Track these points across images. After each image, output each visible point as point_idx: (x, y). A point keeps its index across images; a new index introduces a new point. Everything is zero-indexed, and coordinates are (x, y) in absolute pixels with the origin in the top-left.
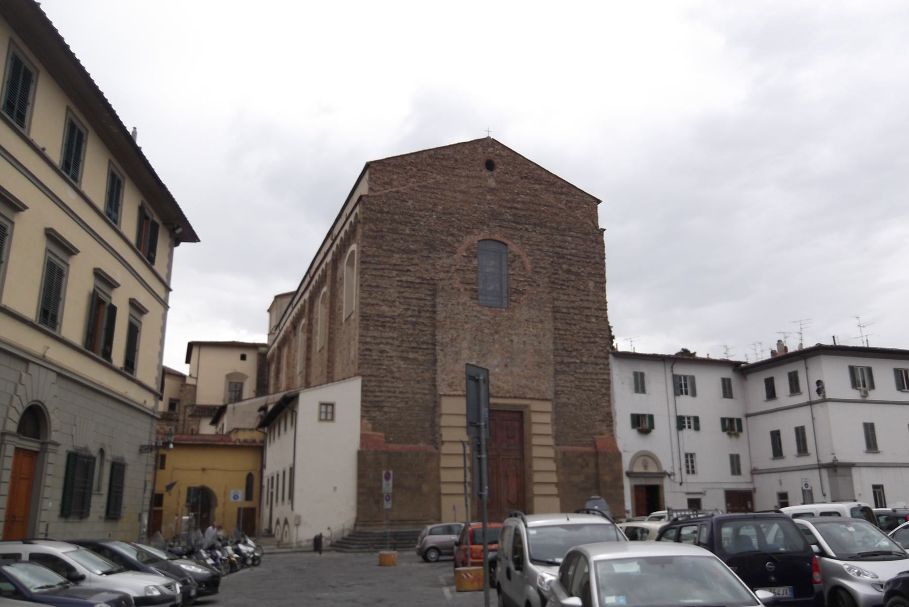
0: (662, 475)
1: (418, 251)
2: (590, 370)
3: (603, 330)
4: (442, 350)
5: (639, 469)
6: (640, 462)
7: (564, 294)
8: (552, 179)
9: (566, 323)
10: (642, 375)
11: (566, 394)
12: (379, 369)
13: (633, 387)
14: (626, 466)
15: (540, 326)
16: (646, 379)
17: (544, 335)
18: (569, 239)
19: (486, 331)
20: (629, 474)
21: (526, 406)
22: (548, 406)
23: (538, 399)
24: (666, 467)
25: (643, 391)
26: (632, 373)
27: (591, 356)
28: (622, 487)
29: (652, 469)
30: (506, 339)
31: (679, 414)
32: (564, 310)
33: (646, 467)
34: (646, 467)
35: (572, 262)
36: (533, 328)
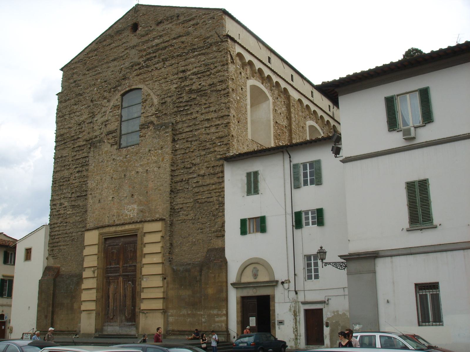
0: (273, 284)
1: (85, 120)
2: (208, 181)
3: (222, 137)
4: (91, 194)
5: (247, 278)
6: (249, 272)
7: (187, 114)
8: (177, 11)
9: (187, 141)
10: (256, 174)
11: (185, 210)
12: (59, 218)
13: (246, 190)
14: (232, 276)
15: (160, 151)
16: (260, 178)
17: (163, 160)
18: (193, 60)
19: (120, 169)
20: (237, 285)
21: (138, 229)
22: (158, 226)
23: (149, 221)
24: (280, 275)
25: (256, 191)
26: (245, 175)
27: (208, 168)
28: (226, 300)
29: (263, 277)
30: (133, 172)
31: (297, 209)
32: (187, 130)
33: (255, 276)
34: (255, 276)
35: (194, 80)
36: (154, 156)
